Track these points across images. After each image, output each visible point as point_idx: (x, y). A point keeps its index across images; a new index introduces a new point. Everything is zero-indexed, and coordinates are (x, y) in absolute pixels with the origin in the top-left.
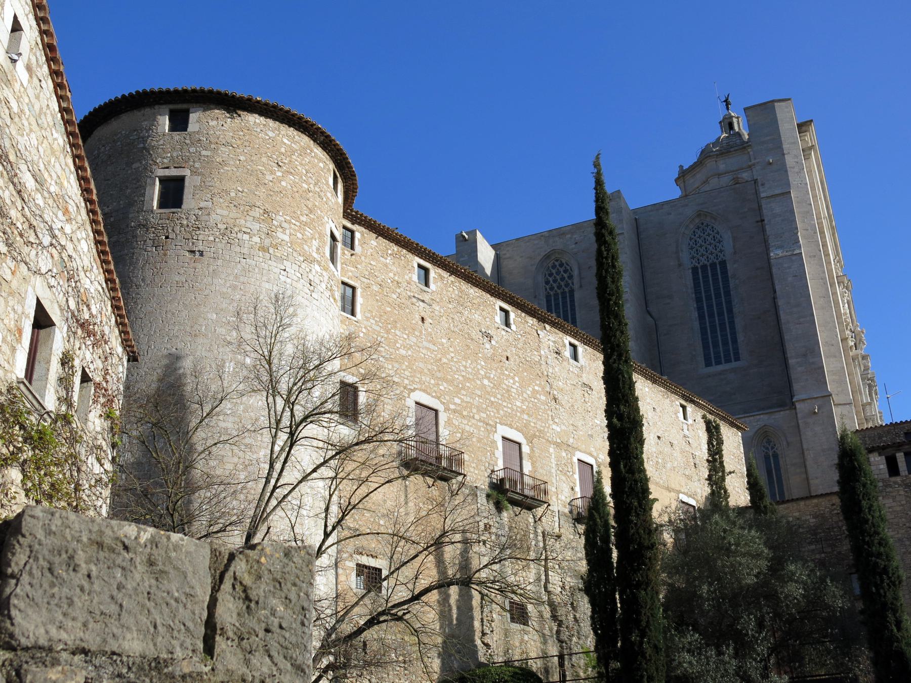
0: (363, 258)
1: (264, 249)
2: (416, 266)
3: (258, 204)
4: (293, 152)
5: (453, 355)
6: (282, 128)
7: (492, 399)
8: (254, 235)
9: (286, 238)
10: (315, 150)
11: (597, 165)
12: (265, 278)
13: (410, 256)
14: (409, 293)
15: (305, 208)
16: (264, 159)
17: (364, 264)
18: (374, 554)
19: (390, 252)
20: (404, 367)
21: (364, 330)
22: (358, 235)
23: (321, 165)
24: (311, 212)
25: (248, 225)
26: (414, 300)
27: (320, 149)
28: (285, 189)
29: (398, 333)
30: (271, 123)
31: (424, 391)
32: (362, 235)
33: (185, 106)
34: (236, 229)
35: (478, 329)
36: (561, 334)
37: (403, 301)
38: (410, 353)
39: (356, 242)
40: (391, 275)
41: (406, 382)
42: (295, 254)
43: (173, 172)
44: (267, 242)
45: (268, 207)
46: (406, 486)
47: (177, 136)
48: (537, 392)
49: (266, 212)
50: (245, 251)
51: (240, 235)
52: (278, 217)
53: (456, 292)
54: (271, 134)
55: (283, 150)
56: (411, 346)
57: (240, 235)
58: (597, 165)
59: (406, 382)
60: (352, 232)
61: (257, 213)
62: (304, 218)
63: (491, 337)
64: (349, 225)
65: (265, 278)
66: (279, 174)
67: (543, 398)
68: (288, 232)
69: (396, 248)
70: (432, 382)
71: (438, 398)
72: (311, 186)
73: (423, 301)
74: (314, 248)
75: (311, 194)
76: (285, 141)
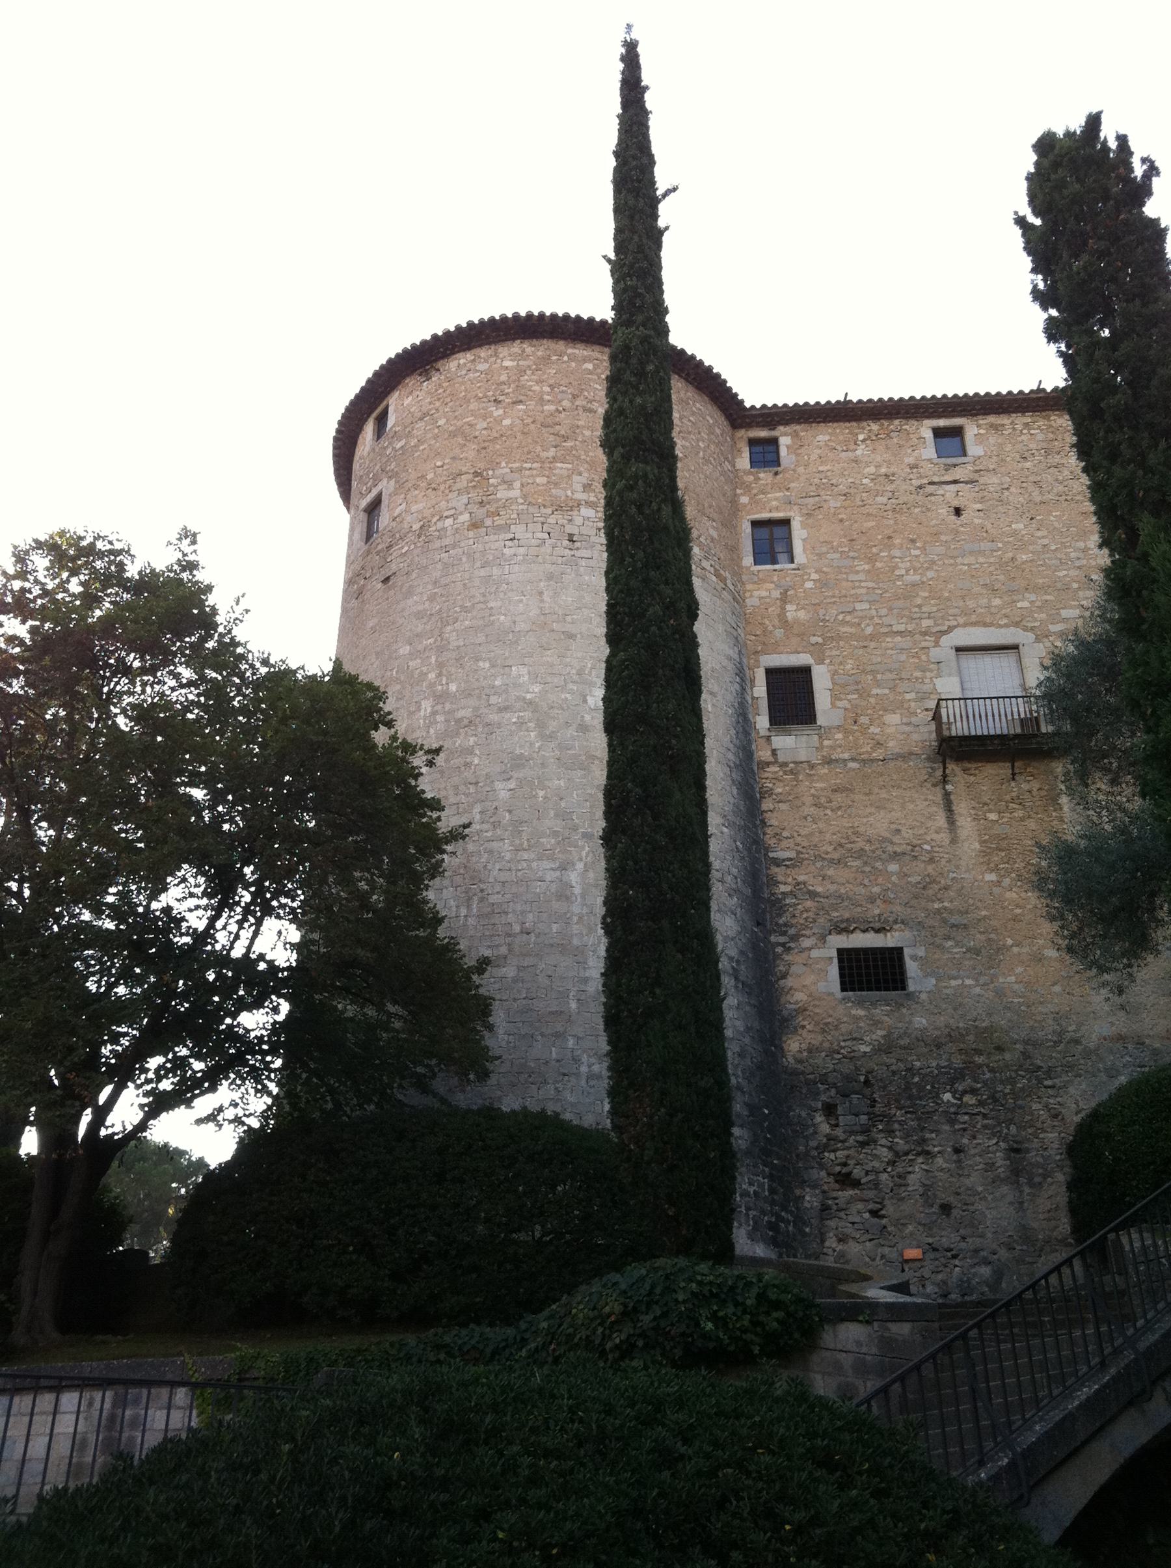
0: (801, 470)
1: (475, 525)
2: (928, 435)
3: (464, 469)
5: (1046, 541)
6: (500, 349)
8: (461, 513)
9: (515, 493)
10: (570, 351)
12: (478, 564)
13: (911, 426)
14: (916, 483)
15: (552, 438)
17: (802, 479)
18: (877, 925)
19: (861, 437)
20: (919, 601)
21: (814, 576)
22: (784, 441)
23: (590, 366)
24: (566, 438)
25: (450, 505)
27: (582, 346)
28: (511, 427)
29: (896, 553)
30: (483, 352)
31: (974, 624)
32: (795, 435)
33: (385, 403)
34: (435, 520)
38: (930, 574)
39: (783, 451)
40: (872, 469)
42: (531, 509)
43: (374, 492)
44: (480, 512)
45: (481, 465)
46: (947, 795)
49: (476, 474)
50: (447, 541)
51: (440, 525)
52: (498, 472)
53: (1041, 437)
55: (503, 378)
56: (933, 562)
57: (440, 525)
59: (926, 623)
60: (774, 442)
61: (463, 481)
62: (552, 452)
64: (763, 433)
65: (478, 564)
66: (501, 412)
68: (517, 484)
69: (875, 427)
70: (997, 602)
71: (1016, 624)
73: (955, 482)
74: (579, 488)
75: (562, 415)
76: (507, 363)
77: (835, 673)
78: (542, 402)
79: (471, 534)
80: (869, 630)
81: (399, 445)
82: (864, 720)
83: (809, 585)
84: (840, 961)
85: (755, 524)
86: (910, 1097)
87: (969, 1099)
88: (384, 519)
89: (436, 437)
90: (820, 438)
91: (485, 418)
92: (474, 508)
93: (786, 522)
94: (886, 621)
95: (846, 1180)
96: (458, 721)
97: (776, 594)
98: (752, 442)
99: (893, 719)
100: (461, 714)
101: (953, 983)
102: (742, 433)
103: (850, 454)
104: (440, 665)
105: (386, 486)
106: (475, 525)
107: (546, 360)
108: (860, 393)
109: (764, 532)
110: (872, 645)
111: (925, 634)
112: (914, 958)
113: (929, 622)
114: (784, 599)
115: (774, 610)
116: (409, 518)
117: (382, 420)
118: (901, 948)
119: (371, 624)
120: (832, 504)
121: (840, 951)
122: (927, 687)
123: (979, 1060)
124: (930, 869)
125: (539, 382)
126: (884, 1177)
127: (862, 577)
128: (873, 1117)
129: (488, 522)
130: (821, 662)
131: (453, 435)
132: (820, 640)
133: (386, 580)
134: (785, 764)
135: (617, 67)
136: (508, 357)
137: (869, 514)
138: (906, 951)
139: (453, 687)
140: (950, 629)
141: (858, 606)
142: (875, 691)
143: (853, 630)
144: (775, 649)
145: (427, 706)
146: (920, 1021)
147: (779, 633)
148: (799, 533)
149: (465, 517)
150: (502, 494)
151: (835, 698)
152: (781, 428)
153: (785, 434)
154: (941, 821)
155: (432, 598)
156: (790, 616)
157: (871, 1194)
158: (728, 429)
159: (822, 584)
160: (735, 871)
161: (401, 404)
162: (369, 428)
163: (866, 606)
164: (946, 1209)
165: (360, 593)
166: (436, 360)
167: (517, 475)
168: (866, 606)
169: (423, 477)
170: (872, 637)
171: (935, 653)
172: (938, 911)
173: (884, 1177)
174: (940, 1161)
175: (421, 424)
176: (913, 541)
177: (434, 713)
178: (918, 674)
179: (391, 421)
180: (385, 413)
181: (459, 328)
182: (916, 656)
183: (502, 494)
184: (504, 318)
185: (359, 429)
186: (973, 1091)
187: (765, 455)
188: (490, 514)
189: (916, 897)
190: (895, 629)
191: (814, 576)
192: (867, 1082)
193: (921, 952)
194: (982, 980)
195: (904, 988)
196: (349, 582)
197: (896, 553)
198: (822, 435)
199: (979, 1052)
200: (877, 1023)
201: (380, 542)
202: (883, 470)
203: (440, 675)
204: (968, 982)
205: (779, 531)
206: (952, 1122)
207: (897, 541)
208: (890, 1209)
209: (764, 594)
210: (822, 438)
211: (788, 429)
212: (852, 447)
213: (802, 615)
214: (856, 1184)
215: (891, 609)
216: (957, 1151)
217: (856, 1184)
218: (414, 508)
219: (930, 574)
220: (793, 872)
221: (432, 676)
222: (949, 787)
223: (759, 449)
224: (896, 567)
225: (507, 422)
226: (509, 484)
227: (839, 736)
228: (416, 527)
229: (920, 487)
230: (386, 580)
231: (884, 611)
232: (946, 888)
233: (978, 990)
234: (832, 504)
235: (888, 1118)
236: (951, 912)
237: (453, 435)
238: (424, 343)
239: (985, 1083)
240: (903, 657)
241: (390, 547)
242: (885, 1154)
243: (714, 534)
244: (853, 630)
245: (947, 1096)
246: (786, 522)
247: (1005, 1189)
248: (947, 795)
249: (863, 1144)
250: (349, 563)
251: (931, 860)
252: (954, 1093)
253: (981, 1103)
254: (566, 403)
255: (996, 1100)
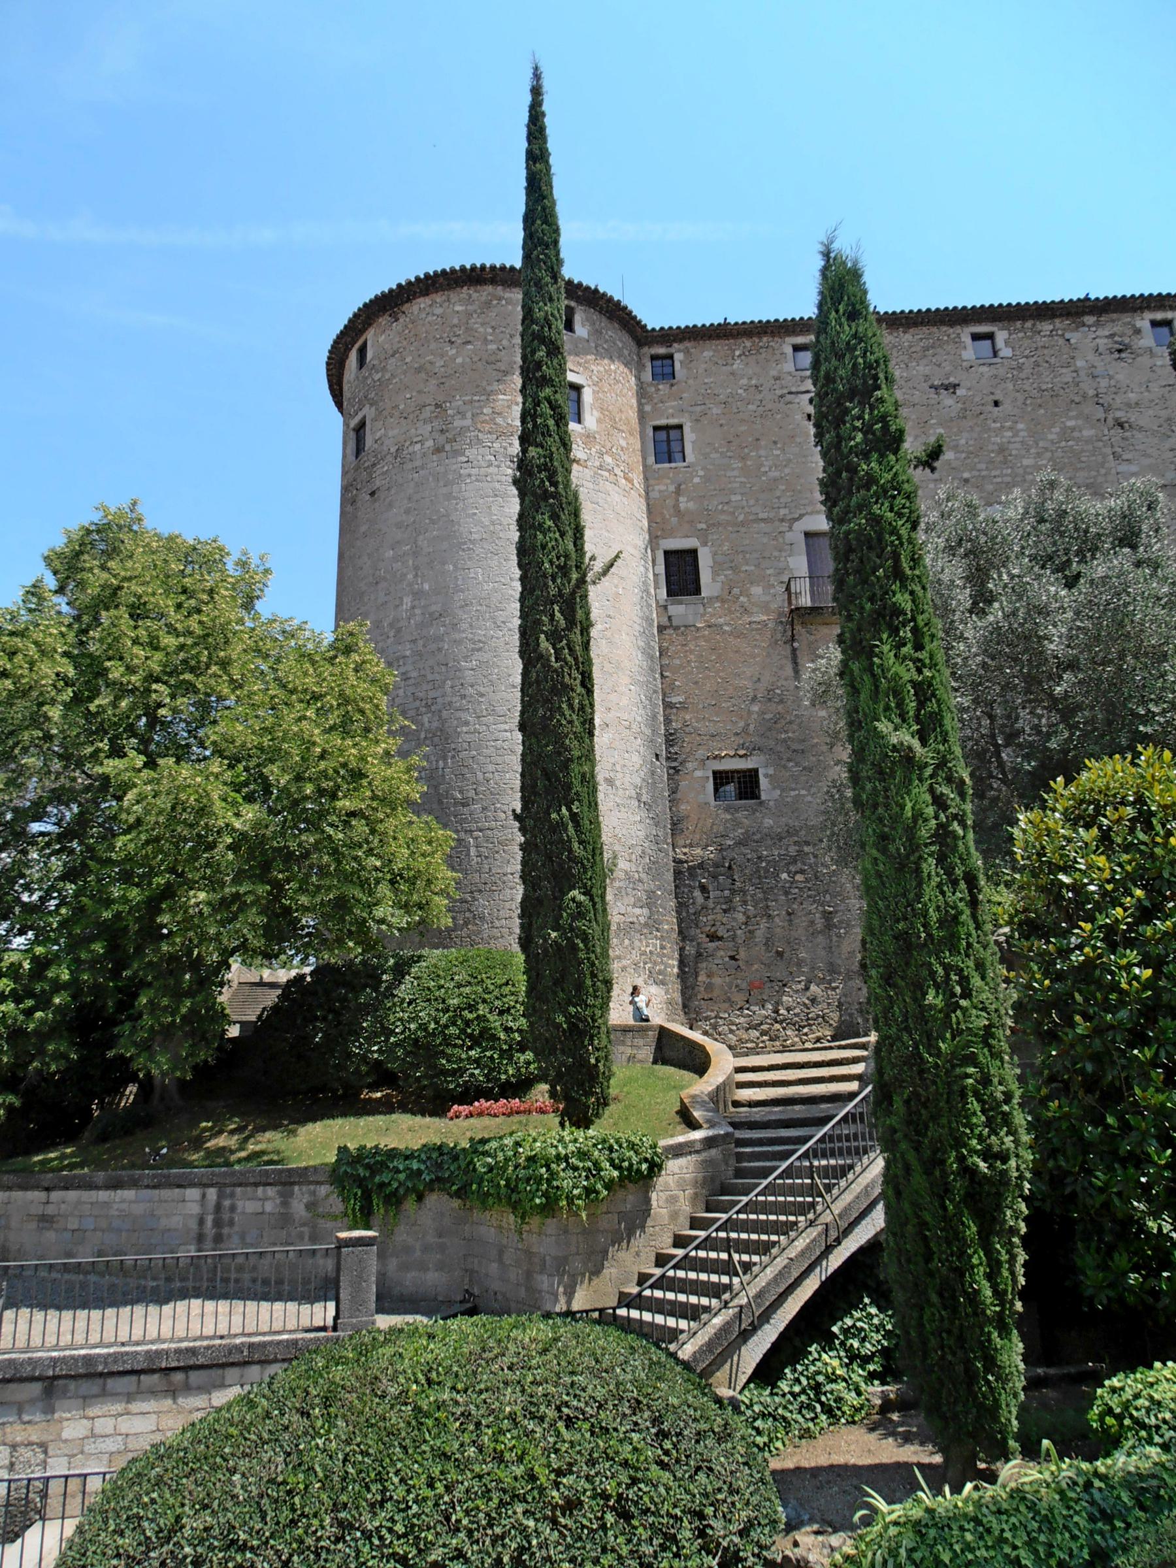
1: (438, 450)
2: (789, 350)
4: (470, 315)
7: (966, 475)
10: (507, 295)
11: (537, 92)
16: (433, 346)
20: (778, 493)
21: (701, 473)
22: (678, 357)
26: (789, 397)
28: (462, 365)
29: (762, 452)
30: (438, 298)
32: (687, 352)
35: (926, 386)
36: (1126, 318)
37: (769, 406)
40: (744, 381)
41: (783, 512)
45: (441, 398)
46: (794, 650)
47: (365, 372)
48: (1073, 429)
50: (418, 463)
54: (438, 311)
55: (455, 321)
58: (537, 92)
59: (783, 512)
60: (671, 357)
63: (956, 386)
64: (662, 350)
67: (1088, 433)
68: (469, 415)
69: (748, 344)
72: (505, 342)
76: (458, 308)
77: (715, 554)
78: (486, 341)
79: (435, 458)
80: (741, 518)
81: (377, 377)
82: (736, 591)
83: (697, 480)
84: (715, 779)
85: (656, 429)
86: (760, 877)
87: (799, 877)
88: (369, 441)
89: (405, 372)
90: (706, 354)
91: (442, 356)
92: (436, 435)
93: (680, 427)
94: (754, 510)
95: (713, 937)
96: (431, 614)
97: (672, 488)
98: (654, 358)
99: (756, 590)
100: (433, 608)
101: (793, 793)
102: (645, 349)
103: (729, 368)
104: (416, 568)
105: (368, 412)
106: (438, 450)
107: (488, 304)
108: (737, 316)
109: (662, 435)
110: (743, 530)
111: (782, 520)
112: (766, 776)
113: (786, 511)
114: (678, 492)
115: (670, 502)
116: (387, 442)
117: (362, 351)
118: (756, 771)
119: (363, 528)
120: (715, 411)
121: (715, 773)
122: (781, 565)
123: (806, 849)
124: (780, 707)
125: (483, 324)
126: (739, 932)
127: (736, 473)
128: (733, 892)
129: (448, 447)
130: (705, 544)
131: (419, 370)
132: (704, 526)
133: (372, 494)
134: (677, 628)
135: (528, 99)
136: (458, 303)
137: (743, 420)
138: (761, 772)
139: (426, 586)
140: (801, 516)
141: (734, 498)
142: (744, 568)
143: (729, 518)
144: (671, 534)
145: (407, 601)
146: (768, 822)
147: (674, 520)
148: (689, 436)
149: (430, 443)
150: (458, 423)
151: (715, 573)
152: (675, 345)
153: (679, 351)
154: (789, 670)
155: (407, 512)
156: (682, 506)
157: (731, 944)
158: (634, 348)
159: (707, 479)
160: (639, 719)
161: (376, 339)
162: (353, 356)
163: (739, 497)
164: (780, 954)
165: (353, 502)
166: (403, 303)
167: (468, 407)
168: (739, 497)
169: (397, 406)
170: (743, 524)
171: (789, 536)
172: (785, 741)
173: (739, 932)
174: (777, 920)
175: (392, 360)
176: (775, 443)
177: (413, 607)
178: (776, 554)
179: (370, 354)
180: (365, 345)
181: (418, 279)
182: (775, 539)
183: (458, 423)
184: (453, 270)
185: (348, 350)
186: (802, 872)
187: (664, 369)
188: (448, 441)
189: (770, 729)
190: (761, 516)
191: (701, 473)
192: (730, 867)
193: (771, 771)
194: (813, 790)
195: (758, 797)
196: (345, 489)
197: (762, 452)
198: (708, 352)
199: (807, 843)
200: (738, 824)
201: (367, 459)
202: (754, 382)
203: (416, 576)
204: (803, 792)
205: (674, 434)
206: (786, 893)
207: (763, 443)
208: (742, 955)
209: (663, 488)
210: (707, 354)
211: (681, 346)
212: (730, 361)
213: (691, 505)
214: (720, 939)
215: (757, 500)
216: (789, 914)
217: (720, 939)
218: (390, 434)
219: (787, 471)
220: (682, 714)
221: (410, 576)
222: (796, 645)
223: (658, 363)
224: (762, 465)
225: (459, 360)
226: (463, 415)
227: (717, 605)
228: (393, 450)
229: (782, 396)
230: (372, 494)
231: (752, 502)
232: (790, 722)
233: (809, 798)
234: (715, 411)
235: (743, 892)
236: (793, 740)
237: (419, 370)
238: (391, 291)
239: (810, 866)
240: (765, 540)
241: (374, 465)
242: (741, 918)
243: (623, 443)
244: (729, 518)
245: (784, 876)
246: (680, 427)
247: (820, 939)
248: (794, 650)
249: (725, 911)
250: (344, 473)
251: (781, 701)
252: (789, 873)
253: (807, 880)
254: (505, 342)
255: (817, 878)
